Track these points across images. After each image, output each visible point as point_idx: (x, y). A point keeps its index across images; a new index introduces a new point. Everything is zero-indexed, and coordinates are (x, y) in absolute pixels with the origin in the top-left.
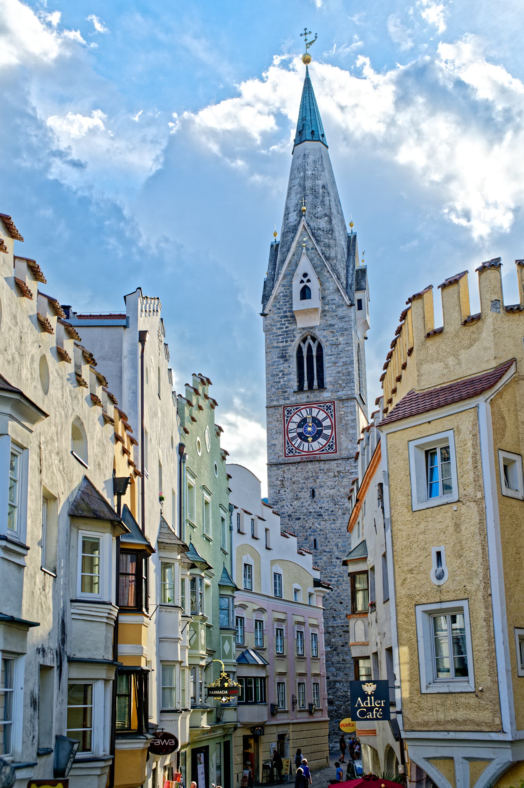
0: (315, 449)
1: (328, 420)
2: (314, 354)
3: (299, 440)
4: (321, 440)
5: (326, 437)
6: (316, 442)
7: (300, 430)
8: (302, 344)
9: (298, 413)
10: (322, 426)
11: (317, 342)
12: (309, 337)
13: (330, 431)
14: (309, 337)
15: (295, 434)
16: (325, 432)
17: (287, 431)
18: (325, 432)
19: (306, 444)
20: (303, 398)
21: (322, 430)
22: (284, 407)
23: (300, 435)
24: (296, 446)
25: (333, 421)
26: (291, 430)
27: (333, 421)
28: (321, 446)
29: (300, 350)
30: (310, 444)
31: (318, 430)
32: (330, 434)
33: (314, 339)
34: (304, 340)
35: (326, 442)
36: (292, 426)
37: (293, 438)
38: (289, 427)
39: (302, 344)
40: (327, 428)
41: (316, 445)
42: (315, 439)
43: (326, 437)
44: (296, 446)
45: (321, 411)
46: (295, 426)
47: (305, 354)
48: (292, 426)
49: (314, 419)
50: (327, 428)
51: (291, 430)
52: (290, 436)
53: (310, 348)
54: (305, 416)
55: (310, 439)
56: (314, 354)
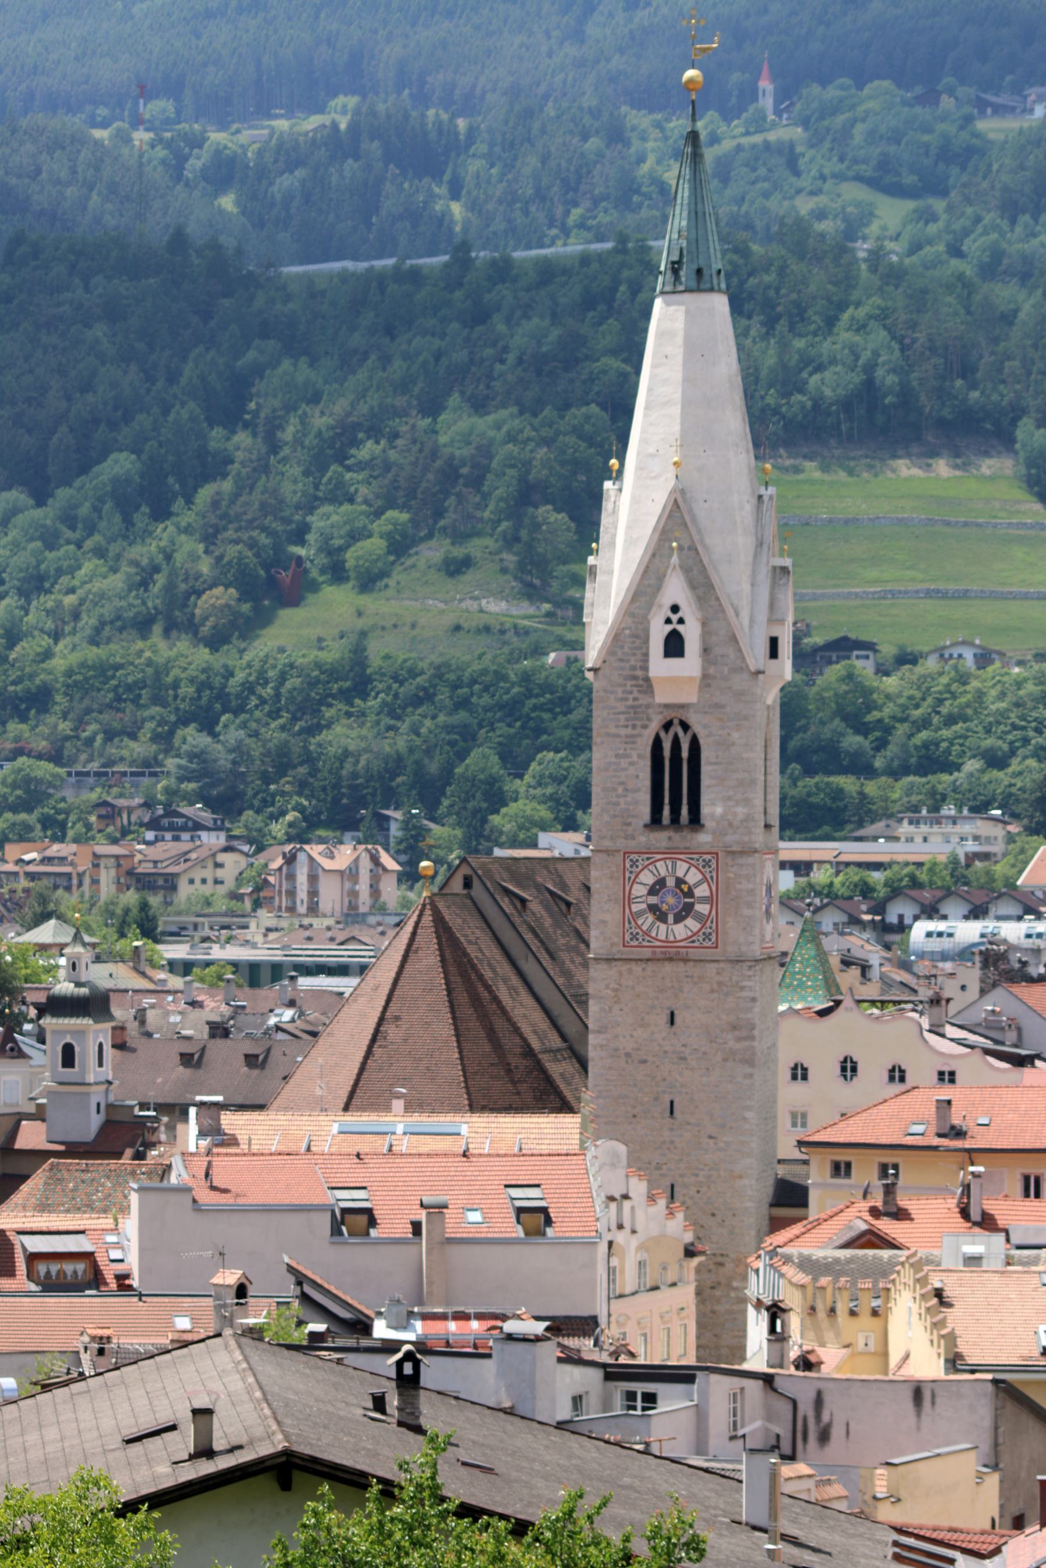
0: (679, 938)
2: (685, 754)
4: (690, 922)
6: (681, 926)
7: (653, 900)
11: (689, 734)
12: (676, 722)
13: (708, 907)
14: (676, 722)
15: (644, 906)
18: (698, 907)
19: (663, 927)
20: (661, 838)
21: (692, 905)
23: (653, 908)
24: (645, 928)
31: (685, 904)
33: (685, 727)
34: (667, 726)
37: (640, 913)
39: (662, 734)
40: (703, 900)
42: (678, 919)
44: (645, 928)
45: (693, 870)
46: (644, 891)
48: (639, 891)
49: (680, 882)
50: (703, 900)
55: (671, 918)
56: (685, 754)
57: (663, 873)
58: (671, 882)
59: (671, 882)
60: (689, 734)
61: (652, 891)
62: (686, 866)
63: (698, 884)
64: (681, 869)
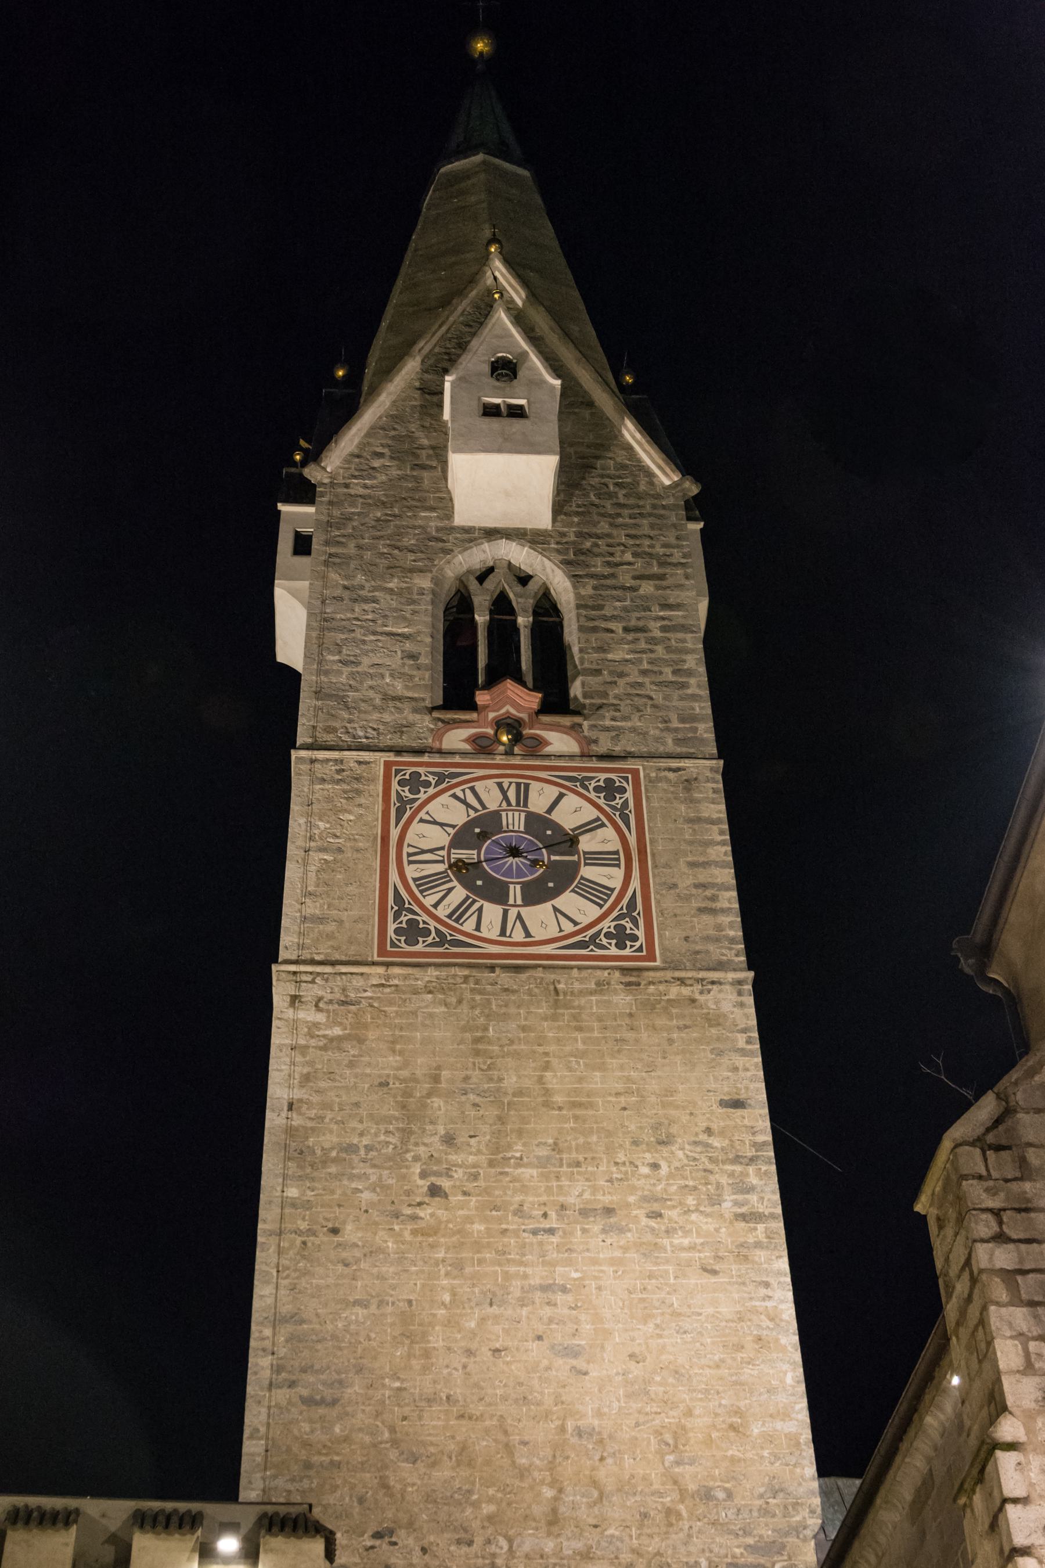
1: (609, 832)
3: (460, 893)
4: (568, 901)
5: (595, 892)
6: (545, 909)
13: (619, 874)
16: (588, 872)
19: (492, 912)
21: (575, 867)
22: (388, 765)
24: (442, 912)
26: (423, 852)
27: (632, 839)
30: (513, 913)
31: (552, 865)
32: (617, 884)
36: (426, 836)
37: (426, 883)
38: (410, 837)
42: (535, 894)
43: (595, 892)
44: (442, 912)
46: (440, 838)
48: (426, 836)
49: (537, 823)
51: (423, 852)
52: (412, 872)
54: (492, 806)
55: (515, 893)
57: (493, 800)
58: (515, 821)
59: (515, 821)
61: (462, 837)
62: (555, 791)
64: (540, 798)
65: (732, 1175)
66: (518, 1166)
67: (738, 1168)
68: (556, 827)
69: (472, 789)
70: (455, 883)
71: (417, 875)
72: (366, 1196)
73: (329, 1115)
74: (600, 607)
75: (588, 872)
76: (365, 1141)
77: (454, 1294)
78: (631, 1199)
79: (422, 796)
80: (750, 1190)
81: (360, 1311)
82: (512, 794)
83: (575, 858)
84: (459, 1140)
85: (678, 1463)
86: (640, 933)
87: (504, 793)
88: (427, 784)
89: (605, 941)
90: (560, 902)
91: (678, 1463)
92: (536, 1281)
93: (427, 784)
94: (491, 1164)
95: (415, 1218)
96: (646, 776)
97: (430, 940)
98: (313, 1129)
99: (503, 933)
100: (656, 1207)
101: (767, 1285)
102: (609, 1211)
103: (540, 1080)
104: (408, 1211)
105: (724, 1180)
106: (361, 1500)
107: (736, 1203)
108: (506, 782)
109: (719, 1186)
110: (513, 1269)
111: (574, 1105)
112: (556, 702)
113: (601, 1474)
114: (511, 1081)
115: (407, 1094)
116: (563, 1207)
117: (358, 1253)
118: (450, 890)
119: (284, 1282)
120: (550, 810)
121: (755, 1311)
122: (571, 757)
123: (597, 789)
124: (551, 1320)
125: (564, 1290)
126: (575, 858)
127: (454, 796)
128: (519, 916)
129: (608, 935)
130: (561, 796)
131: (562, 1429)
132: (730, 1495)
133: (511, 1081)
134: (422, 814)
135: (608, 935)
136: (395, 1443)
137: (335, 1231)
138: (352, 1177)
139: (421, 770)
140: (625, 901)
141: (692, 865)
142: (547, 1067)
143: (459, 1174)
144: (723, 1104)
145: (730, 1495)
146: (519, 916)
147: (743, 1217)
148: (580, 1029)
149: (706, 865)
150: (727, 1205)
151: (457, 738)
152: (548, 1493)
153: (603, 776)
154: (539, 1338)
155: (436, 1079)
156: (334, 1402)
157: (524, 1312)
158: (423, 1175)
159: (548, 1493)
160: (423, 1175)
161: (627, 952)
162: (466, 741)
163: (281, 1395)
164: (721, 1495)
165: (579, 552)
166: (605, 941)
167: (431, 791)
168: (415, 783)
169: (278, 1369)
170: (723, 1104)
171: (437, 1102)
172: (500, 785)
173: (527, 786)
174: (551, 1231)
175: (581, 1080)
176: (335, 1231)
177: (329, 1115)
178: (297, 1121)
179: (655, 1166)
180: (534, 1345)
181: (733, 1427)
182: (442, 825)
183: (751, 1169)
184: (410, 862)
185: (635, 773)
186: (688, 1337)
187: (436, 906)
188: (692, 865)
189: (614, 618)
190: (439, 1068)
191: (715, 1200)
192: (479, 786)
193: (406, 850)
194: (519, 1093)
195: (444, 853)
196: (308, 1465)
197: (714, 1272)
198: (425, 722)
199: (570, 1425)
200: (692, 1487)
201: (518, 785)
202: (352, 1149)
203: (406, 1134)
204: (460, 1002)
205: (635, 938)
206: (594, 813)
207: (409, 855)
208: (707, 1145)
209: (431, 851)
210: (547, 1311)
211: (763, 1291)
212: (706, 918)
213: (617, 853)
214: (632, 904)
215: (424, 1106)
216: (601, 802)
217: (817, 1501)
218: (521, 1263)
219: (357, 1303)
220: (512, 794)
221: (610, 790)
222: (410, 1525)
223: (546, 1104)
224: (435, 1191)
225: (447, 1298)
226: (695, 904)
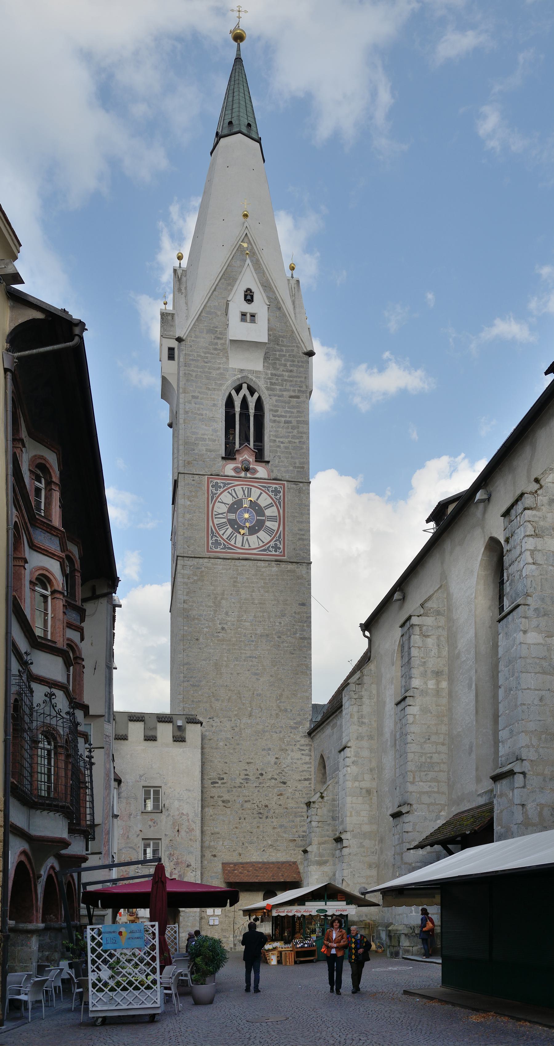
0: (252, 547)
1: (274, 508)
3: (230, 530)
4: (261, 534)
7: (232, 516)
8: (234, 393)
9: (229, 490)
10: (264, 515)
11: (256, 396)
12: (245, 386)
13: (276, 524)
14: (245, 386)
17: (209, 514)
18: (268, 524)
23: (232, 523)
24: (225, 537)
25: (281, 512)
26: (219, 514)
27: (281, 512)
28: (261, 544)
29: (230, 402)
30: (245, 537)
31: (257, 520)
33: (252, 391)
34: (238, 389)
35: (269, 538)
37: (221, 526)
38: (215, 509)
41: (253, 539)
42: (253, 531)
43: (269, 531)
45: (264, 494)
46: (224, 509)
47: (238, 409)
49: (254, 505)
51: (219, 514)
52: (216, 521)
53: (244, 402)
54: (240, 497)
60: (256, 396)
62: (259, 491)
63: (270, 506)
65: (300, 626)
66: (245, 622)
67: (301, 624)
68: (259, 506)
69: (234, 490)
70: (229, 526)
71: (218, 523)
72: (205, 629)
73: (195, 605)
74: (277, 411)
75: (268, 524)
76: (205, 613)
77: (228, 658)
78: (274, 632)
79: (219, 492)
80: (304, 630)
81: (204, 662)
82: (246, 492)
83: (264, 518)
84: (229, 614)
85: (280, 703)
86: (281, 547)
87: (244, 491)
88: (220, 487)
89: (271, 549)
90: (259, 534)
91: (280, 703)
92: (248, 655)
93: (220, 487)
94: (238, 621)
95: (218, 636)
96: (287, 486)
97: (221, 547)
98: (191, 609)
99: (242, 546)
100: (280, 635)
101: (306, 657)
102: (267, 635)
103: (251, 596)
104: (216, 634)
105: (297, 627)
106: (206, 710)
107: (300, 634)
108: (244, 487)
109: (296, 629)
110: (242, 651)
111: (260, 603)
112: (260, 457)
113: (262, 705)
114: (243, 596)
115: (216, 598)
116: (256, 634)
117: (203, 646)
118: (227, 529)
119: (185, 654)
120: (257, 499)
121: (302, 664)
122: (265, 479)
123: (272, 491)
124: (252, 666)
125: (256, 658)
126: (264, 518)
127: (228, 492)
128: (247, 539)
129: (272, 547)
130: (261, 493)
131: (253, 694)
132: (291, 711)
133: (243, 596)
134: (219, 499)
135: (272, 547)
136: (214, 696)
137: (197, 639)
138: (202, 624)
139: (218, 481)
140: (278, 535)
141: (298, 522)
142: (253, 591)
143: (229, 624)
144: (300, 604)
145: (291, 711)
146: (247, 539)
147: (301, 638)
148: (263, 579)
149: (302, 522)
150: (298, 635)
151: (229, 468)
152: (249, 709)
153: (274, 486)
154: (249, 670)
155: (223, 594)
156: (198, 686)
157: (245, 663)
158: (220, 624)
159: (249, 709)
160: (220, 624)
161: (277, 553)
162: (232, 469)
163: (186, 684)
164: (289, 710)
165: (272, 384)
166: (271, 549)
167: (222, 490)
168: (216, 486)
169: (184, 677)
170: (300, 604)
171: (223, 602)
172: (242, 488)
173: (251, 489)
174: (253, 641)
175: (262, 596)
176: (197, 639)
177: (195, 605)
178: (186, 606)
179: (280, 623)
180: (247, 672)
181: (294, 694)
182: (225, 504)
183: (305, 625)
184: (216, 518)
185: (284, 485)
186: (285, 671)
187: (223, 535)
188: (298, 522)
189: (282, 416)
190: (224, 591)
191: (295, 633)
192: (236, 488)
193: (214, 513)
194: (245, 599)
195: (225, 515)
196: (193, 701)
197: (293, 654)
198: (221, 462)
199: (255, 692)
200: (283, 708)
201: (248, 488)
202: (201, 615)
203: (215, 611)
204: (230, 569)
205: (280, 548)
206: (271, 501)
207: (215, 515)
208: (294, 617)
209: (222, 514)
210: (251, 663)
211: (305, 659)
212: (301, 542)
213: (276, 517)
214: (280, 537)
215: (220, 603)
216: (273, 496)
217: (311, 712)
218: (245, 650)
219: (203, 660)
220: (246, 492)
221: (276, 492)
222: (217, 716)
223: (252, 603)
224: (223, 629)
225: (226, 659)
226: (298, 537)
